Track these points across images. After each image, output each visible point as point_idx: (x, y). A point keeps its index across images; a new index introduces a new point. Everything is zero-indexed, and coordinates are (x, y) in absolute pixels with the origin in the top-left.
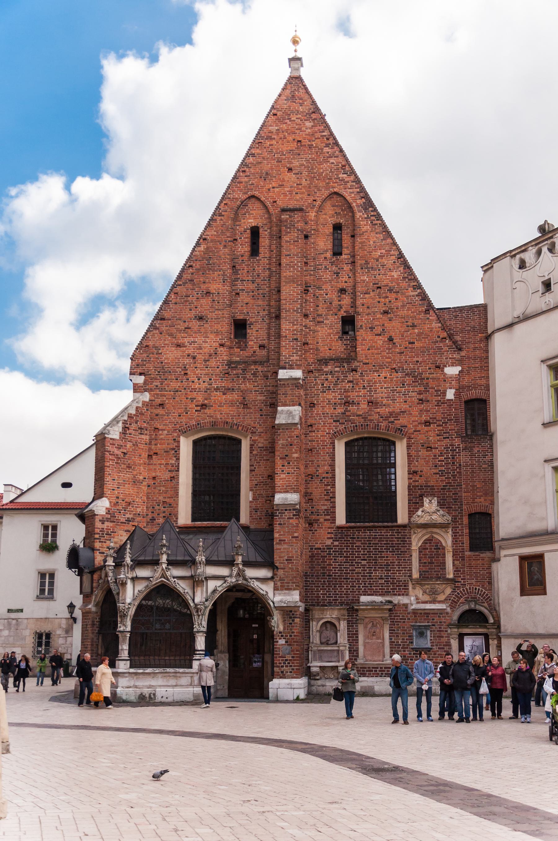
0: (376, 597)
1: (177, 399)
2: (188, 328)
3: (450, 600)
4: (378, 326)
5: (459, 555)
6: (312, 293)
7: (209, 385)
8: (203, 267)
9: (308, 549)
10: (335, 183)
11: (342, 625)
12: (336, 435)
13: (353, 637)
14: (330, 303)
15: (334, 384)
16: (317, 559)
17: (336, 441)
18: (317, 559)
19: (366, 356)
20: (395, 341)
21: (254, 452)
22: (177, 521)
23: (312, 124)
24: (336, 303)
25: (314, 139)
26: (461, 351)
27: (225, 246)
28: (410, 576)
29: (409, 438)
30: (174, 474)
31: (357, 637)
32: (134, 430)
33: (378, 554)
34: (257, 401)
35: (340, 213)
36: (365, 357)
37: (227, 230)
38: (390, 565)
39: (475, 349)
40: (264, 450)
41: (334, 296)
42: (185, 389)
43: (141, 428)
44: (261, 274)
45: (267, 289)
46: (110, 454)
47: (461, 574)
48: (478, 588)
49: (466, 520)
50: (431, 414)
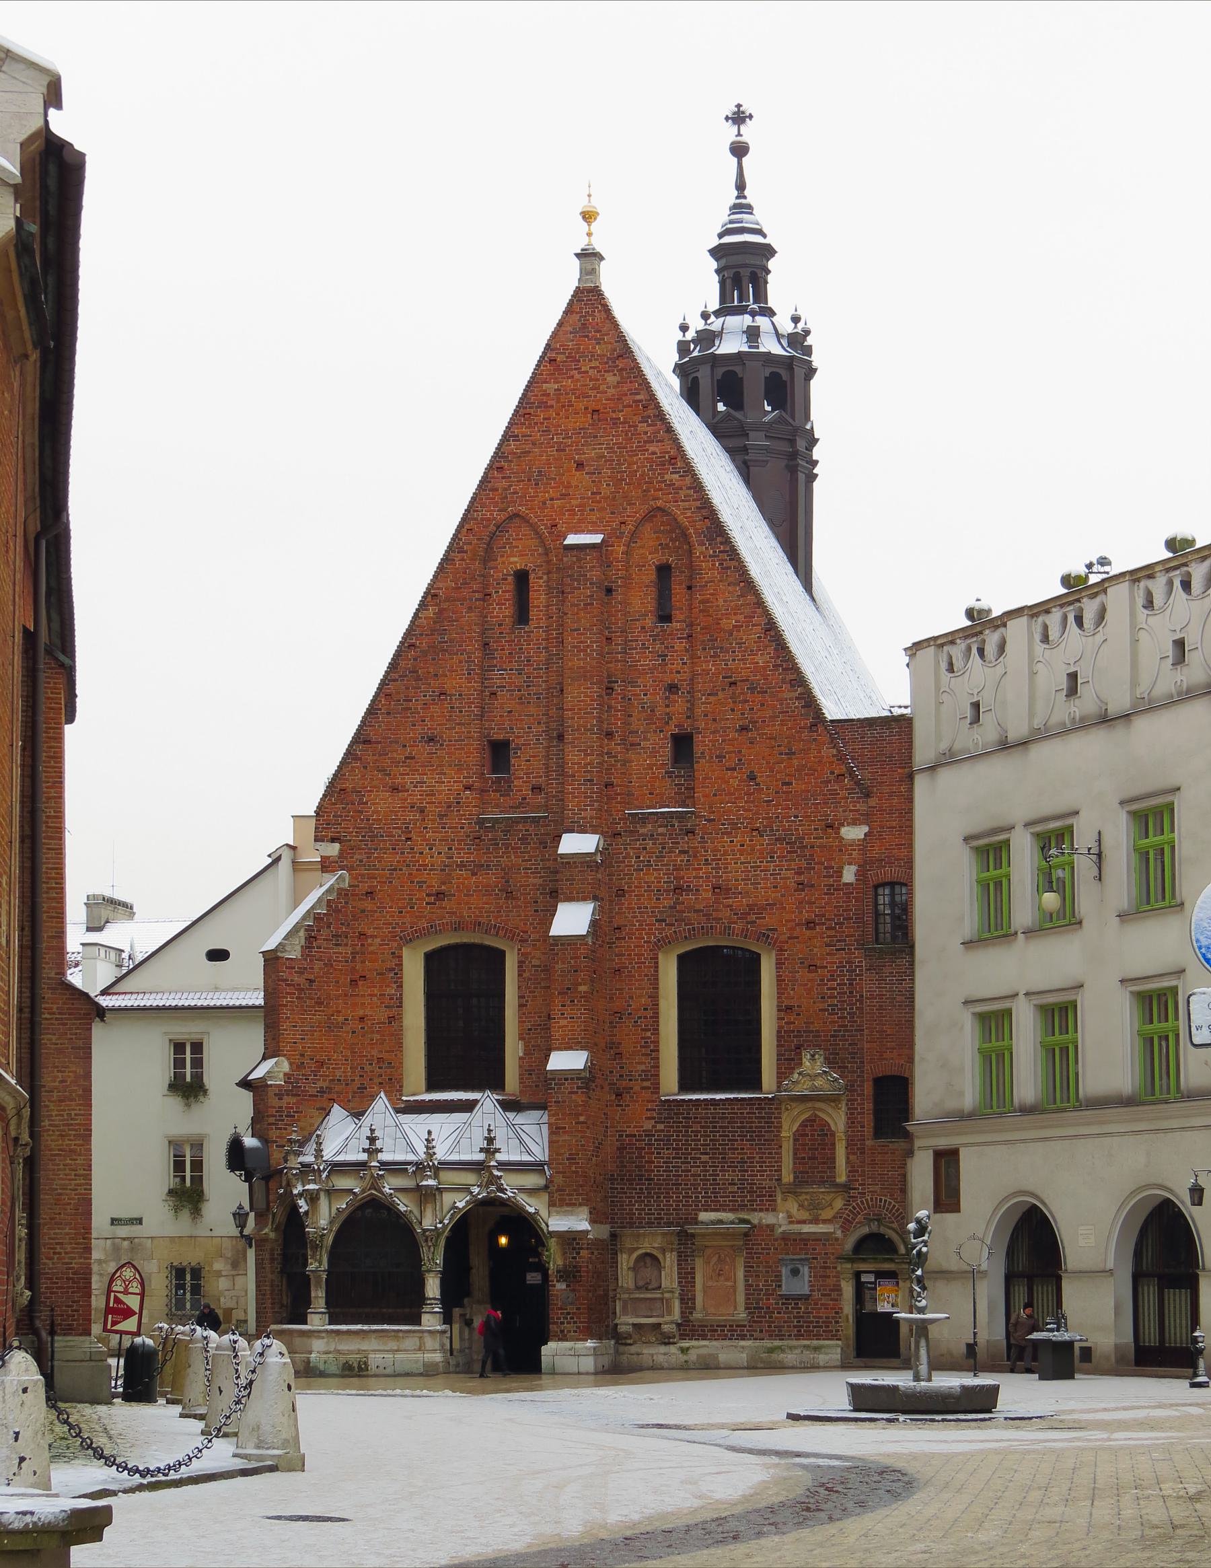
3: (841, 1217)
5: (856, 1145)
6: (619, 694)
9: (615, 1136)
12: (663, 943)
13: (687, 1277)
15: (657, 857)
17: (660, 956)
20: (758, 780)
21: (526, 975)
23: (618, 378)
25: (621, 407)
28: (779, 1180)
30: (394, 1011)
31: (694, 1278)
32: (324, 940)
33: (727, 1145)
35: (667, 545)
37: (473, 579)
38: (746, 1162)
39: (891, 794)
40: (542, 971)
44: (533, 657)
48: (883, 1198)
49: (868, 1089)
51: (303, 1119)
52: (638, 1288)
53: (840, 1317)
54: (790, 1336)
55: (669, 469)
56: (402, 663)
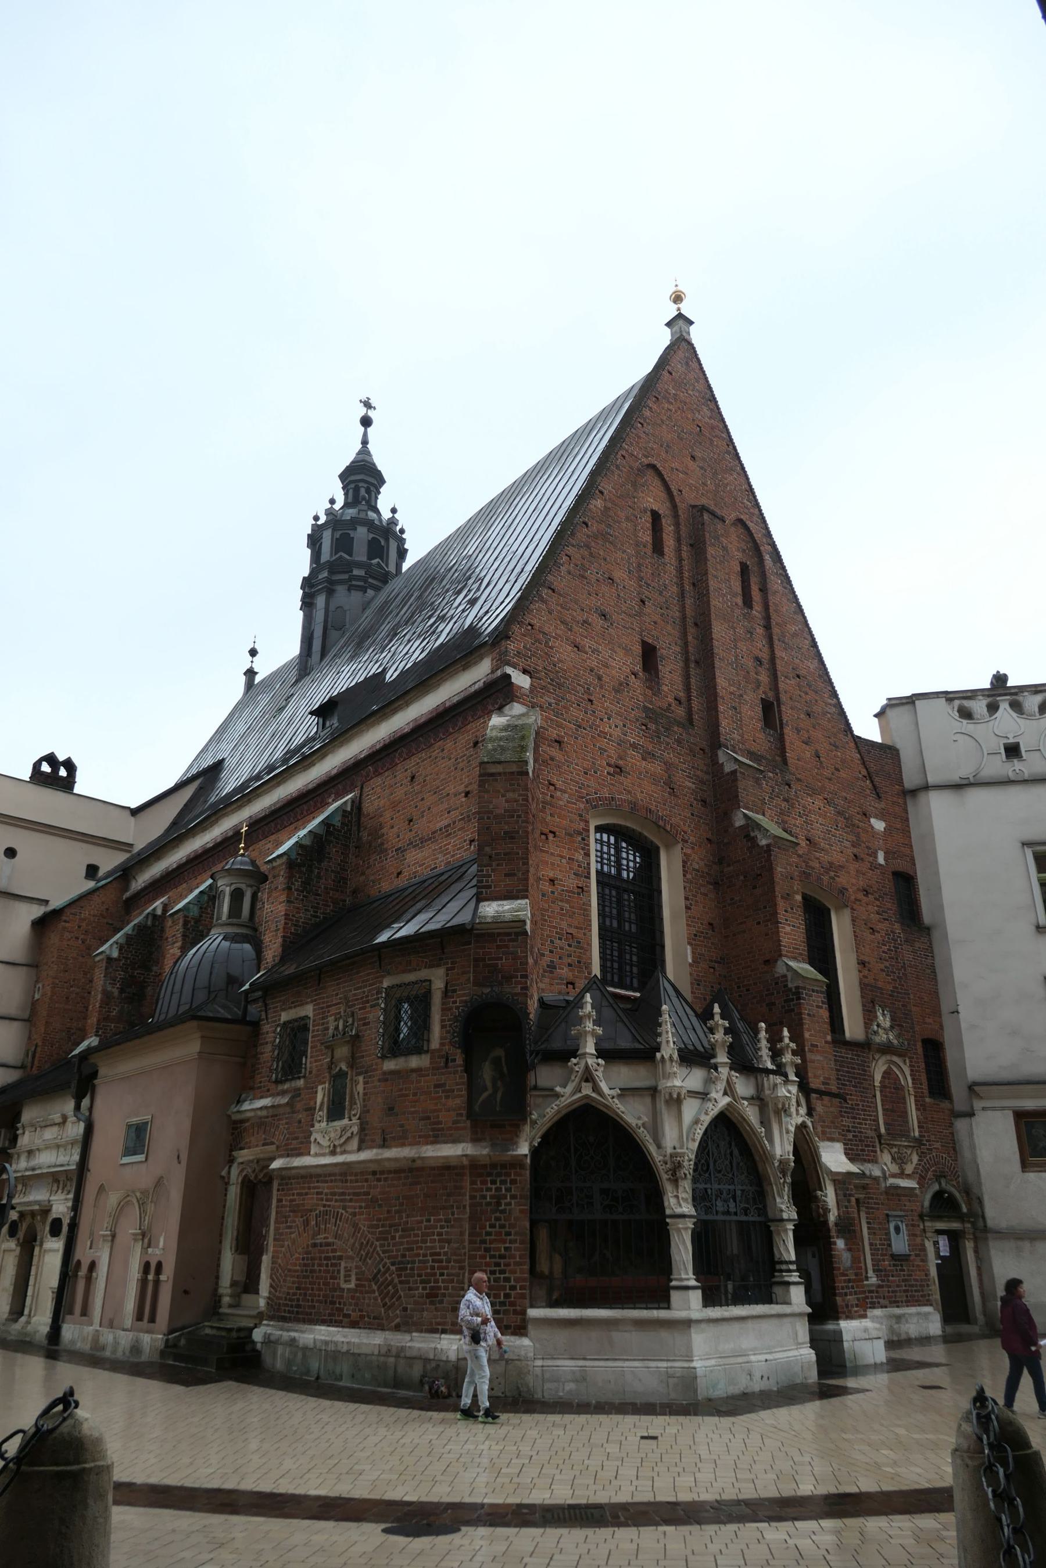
21: (689, 876)
29: (852, 909)
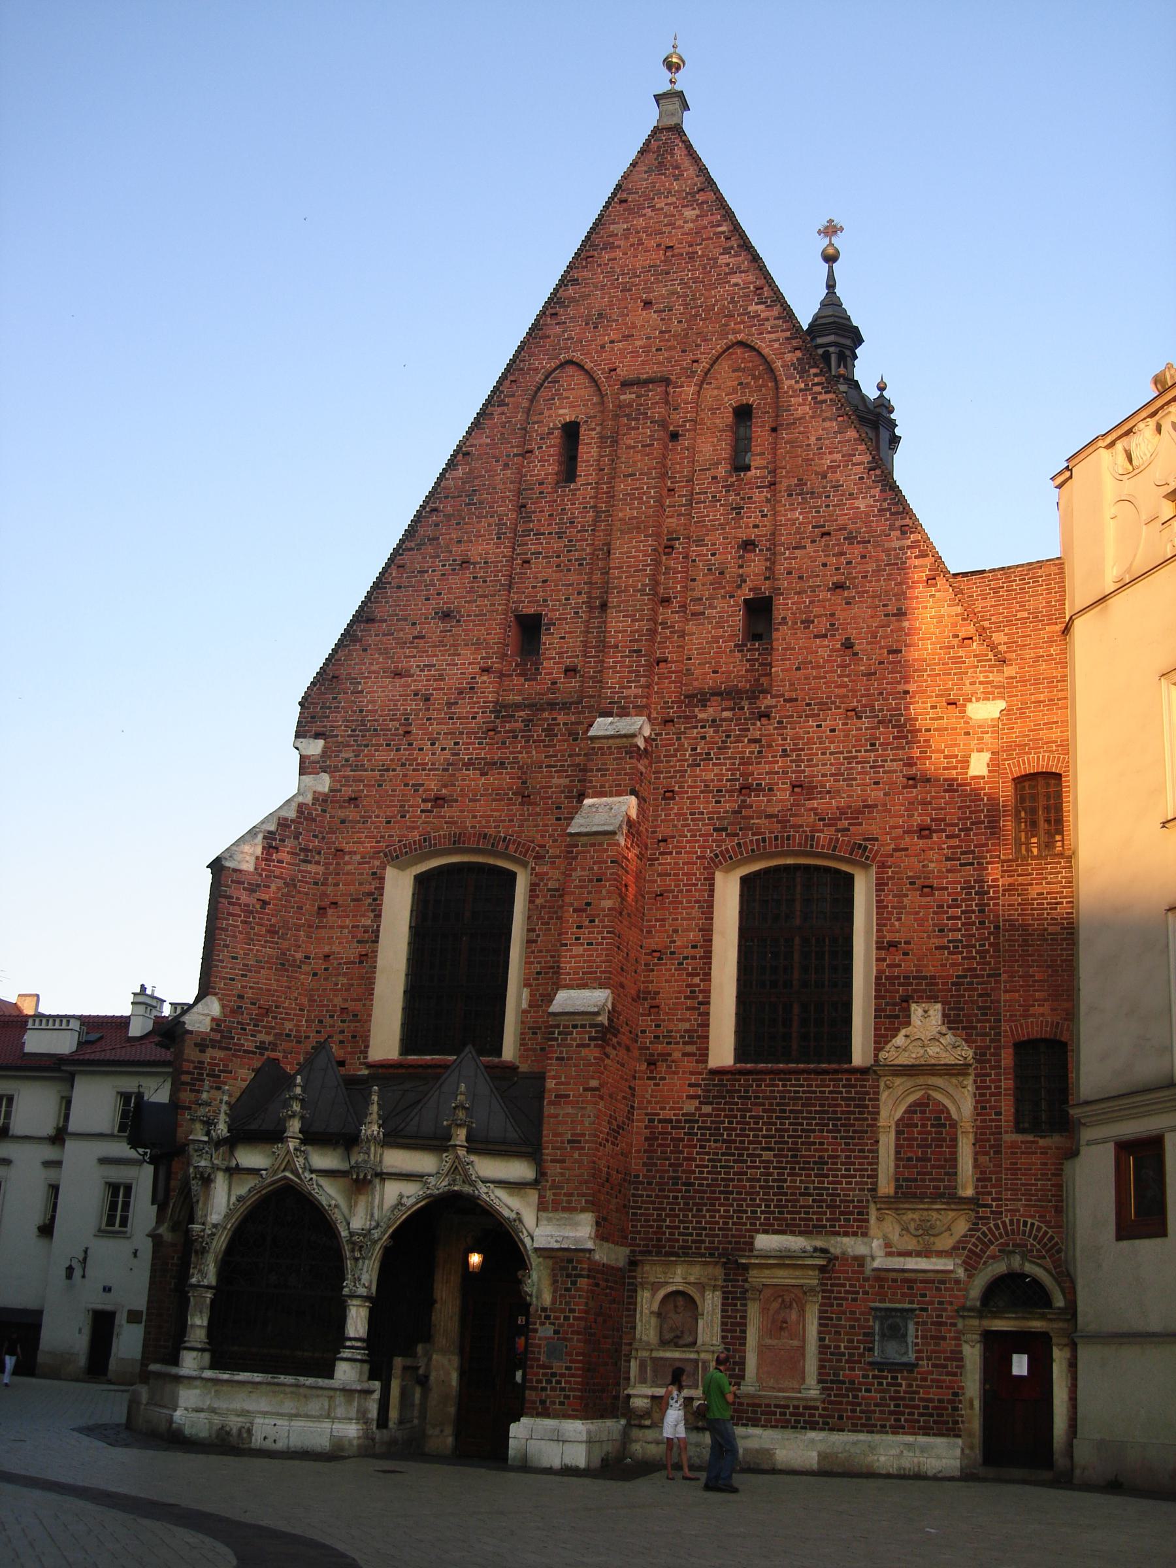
0: (791, 1238)
1: (387, 786)
2: (420, 637)
3: (964, 1248)
4: (820, 616)
5: (989, 1141)
6: (680, 553)
7: (453, 755)
8: (458, 511)
9: (642, 1121)
10: (740, 323)
11: (708, 1302)
13: (734, 1330)
14: (721, 573)
16: (660, 1145)
17: (719, 876)
18: (660, 1145)
19: (792, 684)
20: (857, 648)
21: (539, 901)
22: (366, 1052)
23: (697, 212)
24: (732, 570)
26: (1007, 665)
27: (506, 466)
28: (874, 1190)
29: (883, 866)
31: (744, 1332)
33: (800, 1137)
34: (551, 787)
36: (790, 685)
41: (730, 558)
42: (403, 765)
43: (306, 850)
44: (578, 518)
45: (588, 550)
46: (229, 903)
47: (993, 1186)
48: (1030, 1221)
49: (1007, 1058)
50: (933, 809)
51: (231, 1082)
52: (664, 1343)
53: (960, 1402)
54: (883, 1426)
55: (753, 300)
56: (421, 531)
